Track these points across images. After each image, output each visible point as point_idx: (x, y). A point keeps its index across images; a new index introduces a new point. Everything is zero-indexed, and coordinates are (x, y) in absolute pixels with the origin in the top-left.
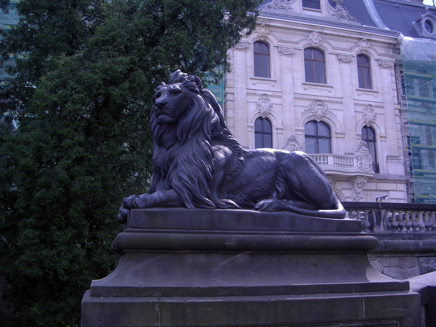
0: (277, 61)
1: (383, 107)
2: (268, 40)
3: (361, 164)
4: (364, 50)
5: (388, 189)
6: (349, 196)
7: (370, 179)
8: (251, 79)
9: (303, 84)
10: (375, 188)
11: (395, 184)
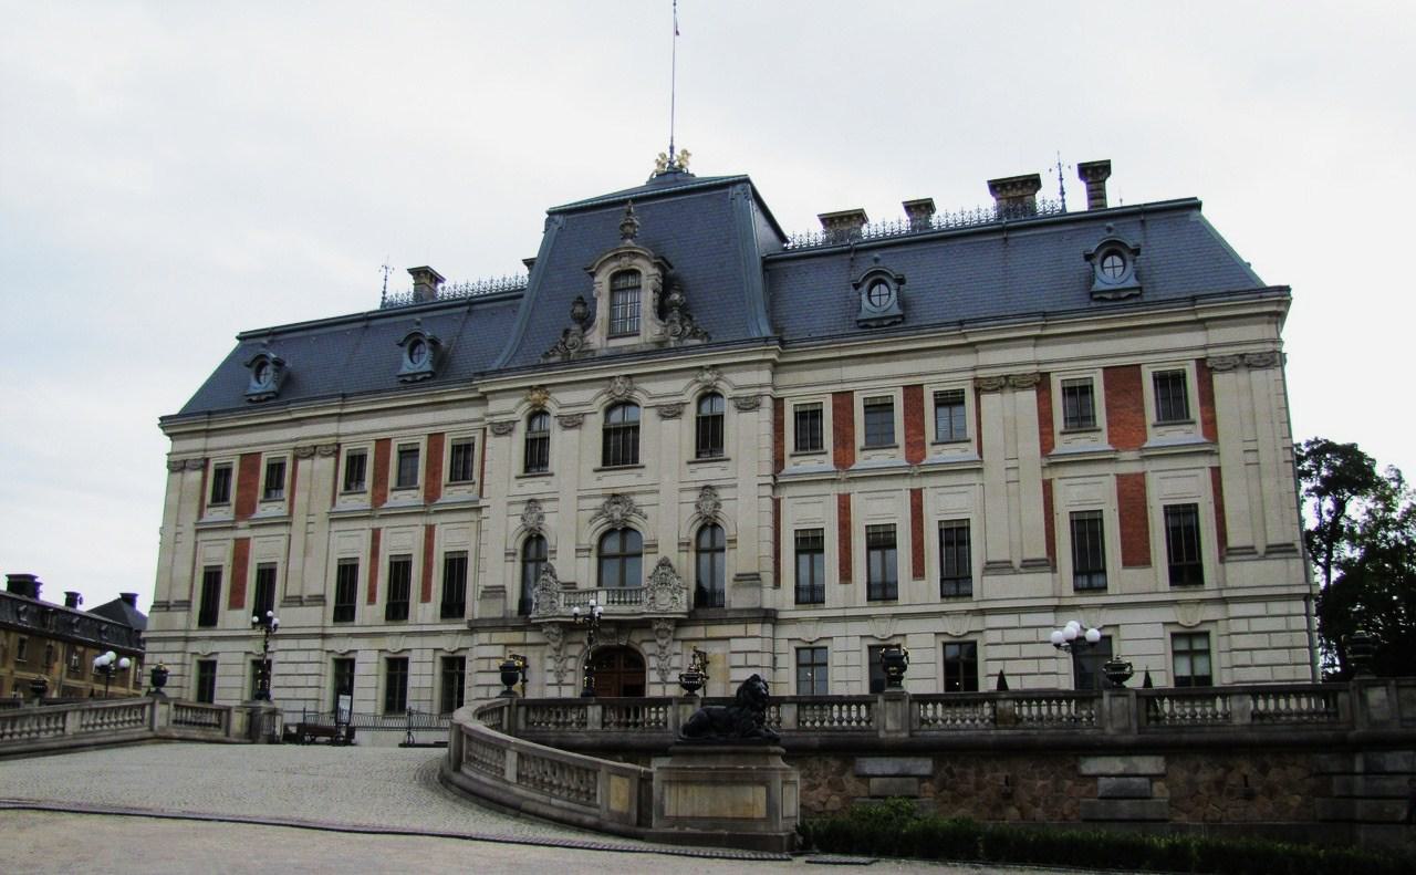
0: (562, 445)
1: (735, 486)
2: (546, 409)
3: (653, 598)
4: (708, 387)
5: (728, 635)
6: (652, 651)
7: (680, 623)
8: (518, 478)
9: (596, 471)
10: (702, 636)
11: (743, 626)
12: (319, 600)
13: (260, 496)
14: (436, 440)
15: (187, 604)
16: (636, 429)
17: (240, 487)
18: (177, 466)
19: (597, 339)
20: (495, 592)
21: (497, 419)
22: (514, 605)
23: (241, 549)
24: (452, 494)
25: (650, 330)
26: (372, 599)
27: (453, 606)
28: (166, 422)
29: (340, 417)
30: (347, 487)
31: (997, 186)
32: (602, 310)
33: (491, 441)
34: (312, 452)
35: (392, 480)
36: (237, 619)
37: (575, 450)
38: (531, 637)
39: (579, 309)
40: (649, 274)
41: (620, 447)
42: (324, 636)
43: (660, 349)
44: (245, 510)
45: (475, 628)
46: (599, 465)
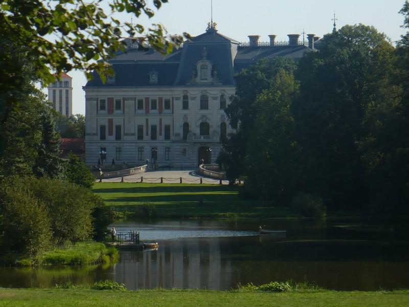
0: (191, 102)
12: (134, 134)
13: (115, 108)
14: (160, 99)
15: (95, 134)
16: (208, 101)
17: (108, 106)
18: (88, 99)
19: (198, 80)
20: (177, 135)
21: (176, 96)
22: (182, 136)
23: (111, 121)
24: (165, 111)
25: (210, 80)
26: (147, 134)
27: (167, 137)
28: (84, 88)
29: (135, 91)
30: (138, 108)
31: (290, 36)
32: (199, 74)
33: (174, 101)
34: (128, 99)
35: (150, 108)
36: (111, 138)
37: (194, 104)
38: (187, 144)
39: (194, 72)
40: (210, 66)
41: (204, 104)
42: (136, 143)
43: (212, 85)
44: (110, 112)
45: (174, 142)
46: (200, 108)
